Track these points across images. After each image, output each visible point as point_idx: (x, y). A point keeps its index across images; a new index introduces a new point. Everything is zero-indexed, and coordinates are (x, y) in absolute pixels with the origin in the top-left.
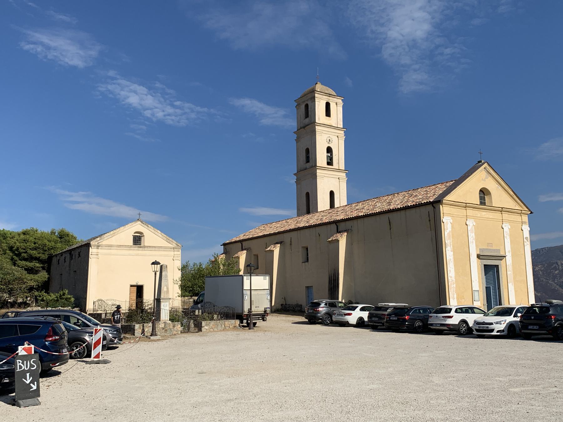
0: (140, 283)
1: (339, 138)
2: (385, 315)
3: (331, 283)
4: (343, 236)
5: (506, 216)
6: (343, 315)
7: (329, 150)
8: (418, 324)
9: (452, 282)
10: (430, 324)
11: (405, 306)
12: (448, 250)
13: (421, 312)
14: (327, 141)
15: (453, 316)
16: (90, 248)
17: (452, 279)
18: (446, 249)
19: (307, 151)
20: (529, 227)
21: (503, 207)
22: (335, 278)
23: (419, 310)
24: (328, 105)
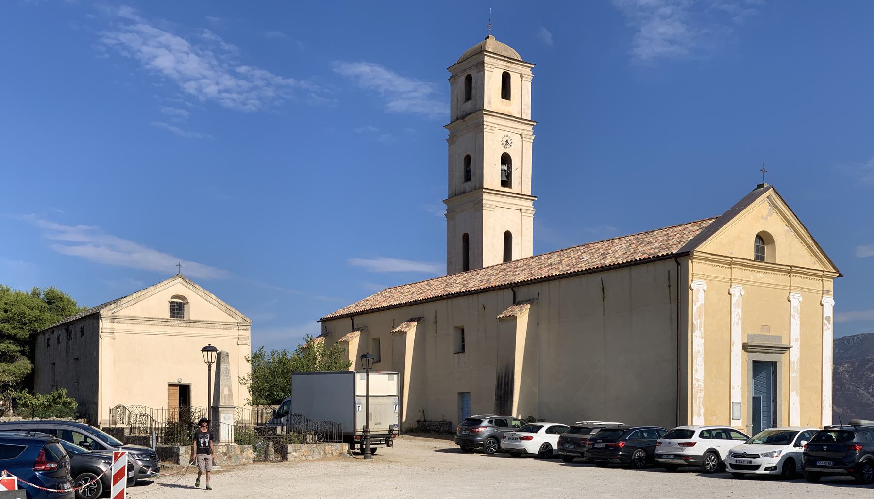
0: (184, 381)
1: (524, 139)
2: (585, 440)
3: (501, 387)
4: (523, 310)
5: (796, 280)
6: (519, 439)
7: (506, 159)
8: (638, 454)
9: (699, 389)
10: (658, 454)
11: (619, 426)
13: (645, 435)
14: (502, 144)
15: (695, 443)
16: (100, 320)
18: (693, 334)
19: (468, 160)
20: (834, 299)
21: (794, 265)
22: (507, 380)
23: (642, 432)
24: (506, 78)
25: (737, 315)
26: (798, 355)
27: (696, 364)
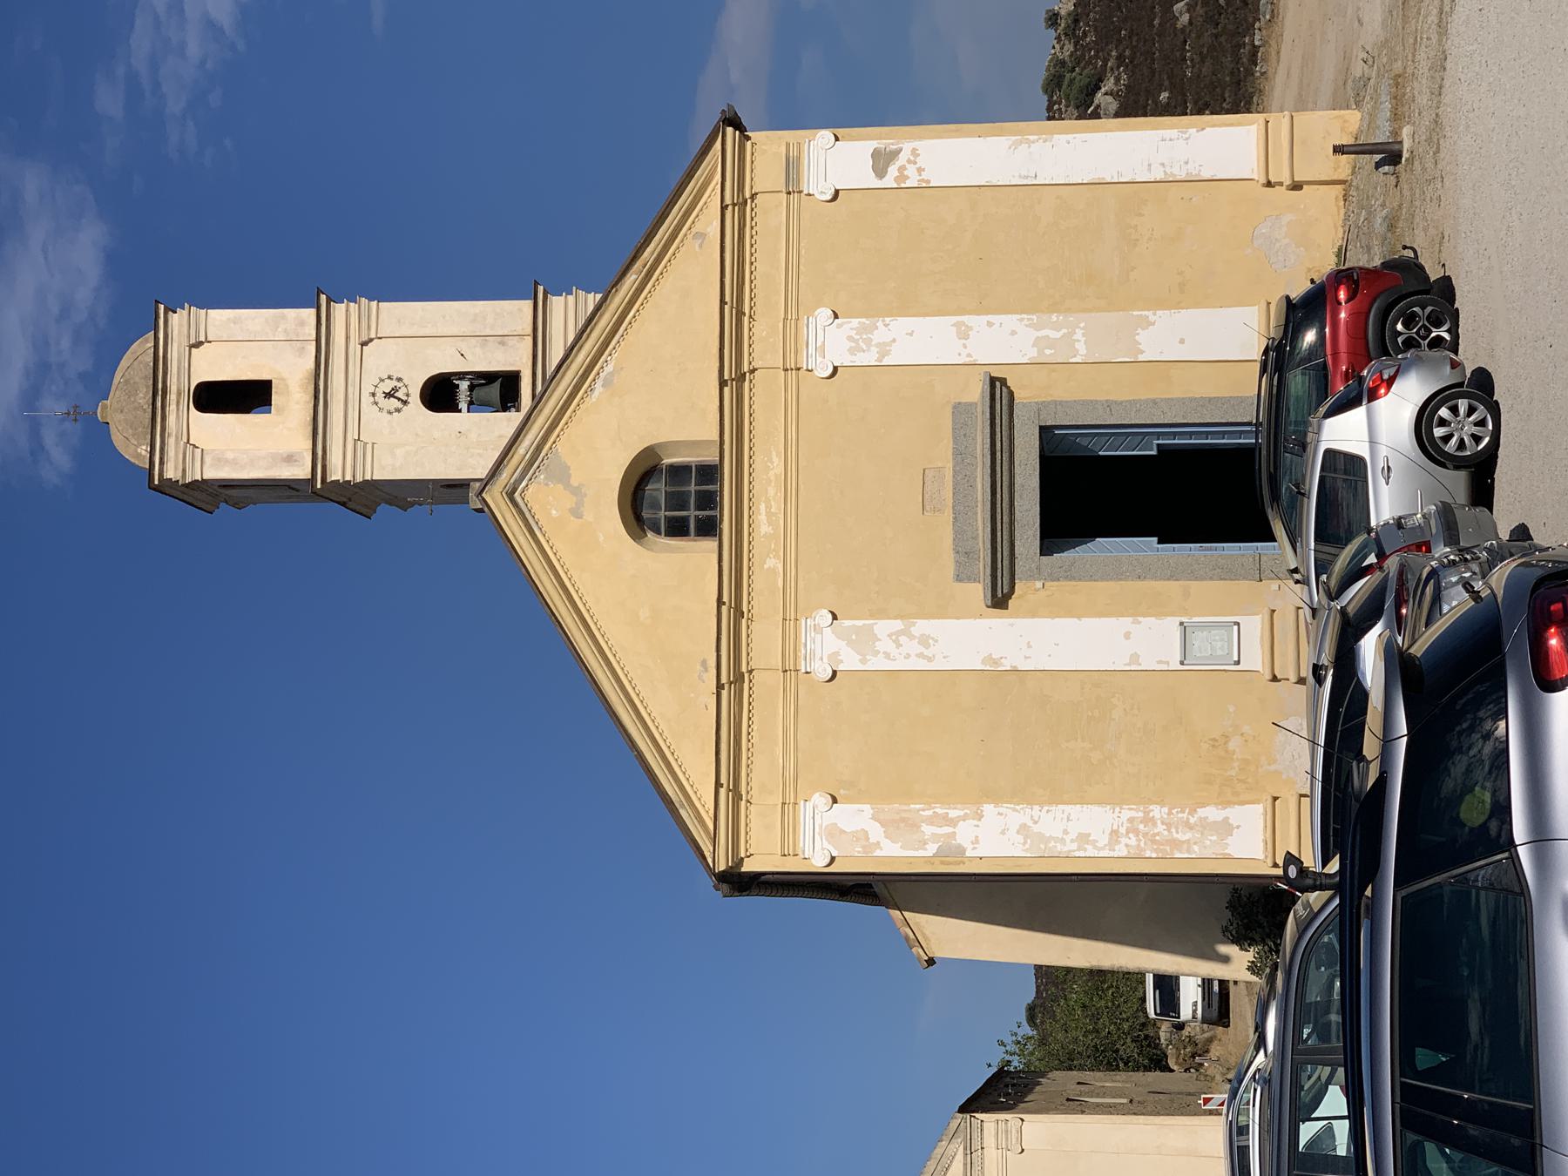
5: (763, 346)
9: (1141, 827)
12: (976, 841)
17: (1123, 830)
25: (899, 645)
26: (1010, 321)
27: (1062, 841)
